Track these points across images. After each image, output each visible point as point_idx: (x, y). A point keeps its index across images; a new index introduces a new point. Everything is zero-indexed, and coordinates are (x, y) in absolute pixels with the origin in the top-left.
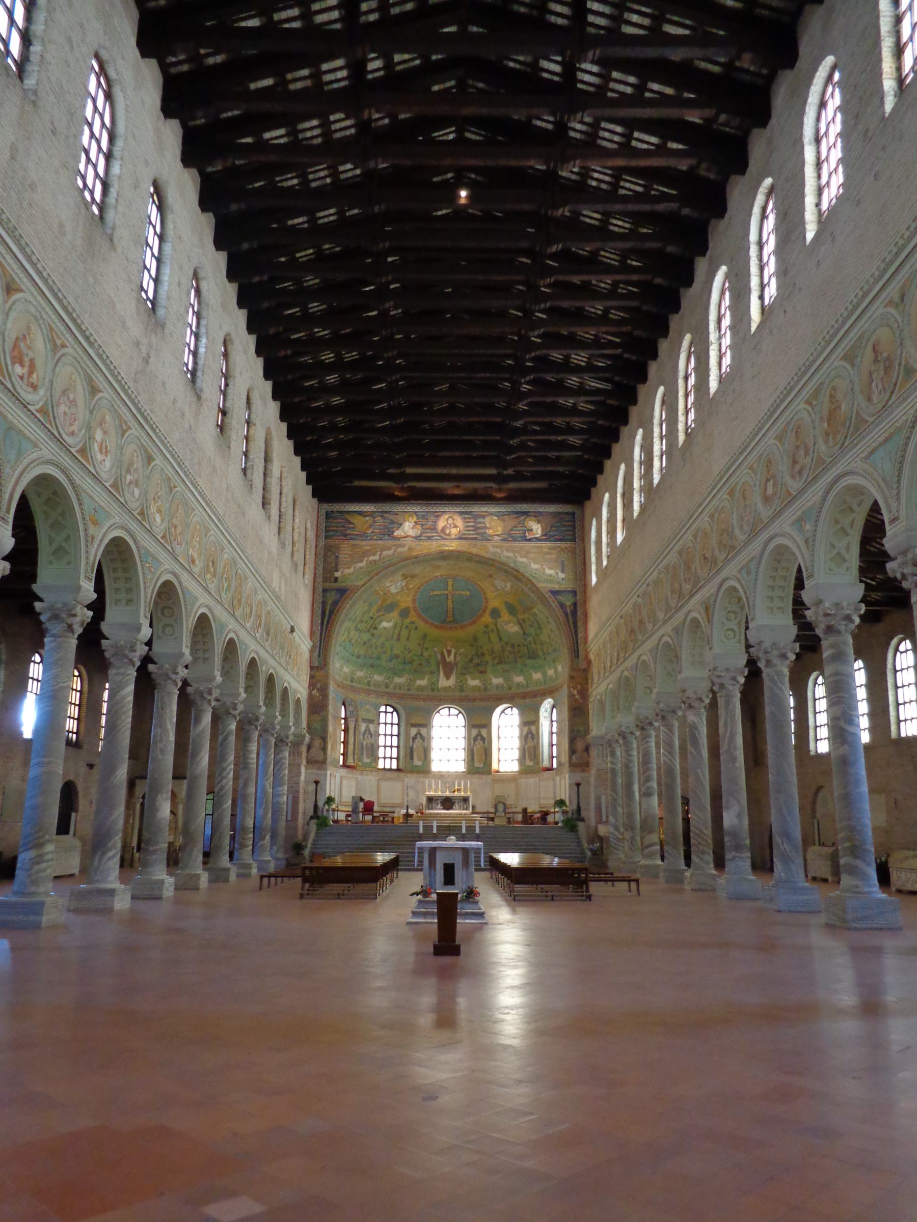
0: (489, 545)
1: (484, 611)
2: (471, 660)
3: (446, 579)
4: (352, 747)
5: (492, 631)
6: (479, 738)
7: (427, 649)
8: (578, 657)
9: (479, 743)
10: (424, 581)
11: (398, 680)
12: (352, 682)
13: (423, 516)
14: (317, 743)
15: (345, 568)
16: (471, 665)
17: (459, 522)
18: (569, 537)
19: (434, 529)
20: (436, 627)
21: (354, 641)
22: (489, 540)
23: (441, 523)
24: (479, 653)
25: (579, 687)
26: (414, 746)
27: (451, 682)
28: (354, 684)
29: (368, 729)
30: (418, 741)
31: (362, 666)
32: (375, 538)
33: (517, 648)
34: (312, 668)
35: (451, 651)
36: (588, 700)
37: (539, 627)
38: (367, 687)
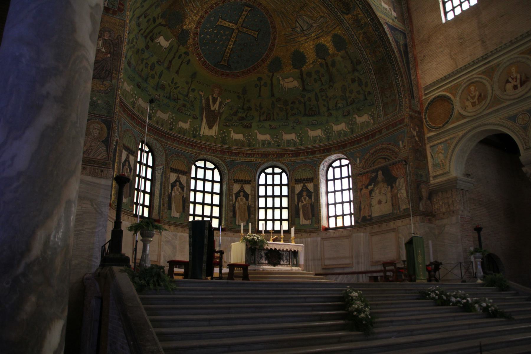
1: (263, 61)
2: (235, 114)
5: (266, 85)
6: (242, 194)
7: (193, 90)
8: (414, 98)
9: (242, 199)
25: (417, 128)
26: (173, 194)
27: (213, 132)
29: (127, 160)
30: (178, 190)
35: (217, 99)
36: (425, 144)
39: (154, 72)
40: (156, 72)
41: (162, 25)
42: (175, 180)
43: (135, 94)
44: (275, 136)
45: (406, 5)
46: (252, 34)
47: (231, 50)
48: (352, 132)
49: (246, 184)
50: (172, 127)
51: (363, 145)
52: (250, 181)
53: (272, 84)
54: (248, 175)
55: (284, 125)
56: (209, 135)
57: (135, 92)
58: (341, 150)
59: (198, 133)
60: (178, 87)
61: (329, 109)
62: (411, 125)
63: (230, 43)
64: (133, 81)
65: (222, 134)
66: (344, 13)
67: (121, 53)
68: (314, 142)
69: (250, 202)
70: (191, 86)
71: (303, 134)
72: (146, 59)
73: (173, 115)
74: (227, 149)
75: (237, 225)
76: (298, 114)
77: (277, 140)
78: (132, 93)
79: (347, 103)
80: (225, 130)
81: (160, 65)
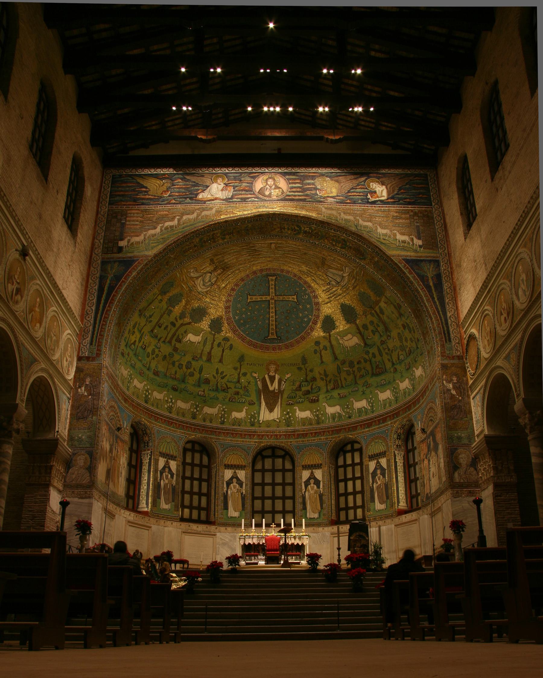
0: (320, 206)
1: (315, 323)
2: (299, 388)
3: (268, 275)
4: (146, 487)
6: (312, 481)
7: (245, 374)
8: (450, 341)
9: (312, 486)
10: (239, 277)
11: (208, 410)
12: (146, 402)
13: (235, 177)
14: (81, 460)
15: (132, 237)
16: (299, 393)
17: (282, 183)
18: (423, 201)
19: (250, 190)
20: (255, 346)
21: (149, 350)
22: (321, 202)
23: (259, 185)
24: (308, 379)
25: (455, 379)
26: (229, 492)
27: (276, 414)
28: (148, 406)
29: (167, 466)
30: (235, 487)
31: (162, 386)
32: (174, 202)
33: (357, 366)
34: (79, 359)
36: (469, 397)
37: (387, 329)
38: (168, 414)
39: (192, 370)
40: (194, 369)
41: (185, 324)
42: (230, 477)
43: (171, 399)
44: (346, 407)
45: (442, 221)
46: (290, 299)
47: (276, 321)
48: (414, 388)
49: (316, 468)
50: (224, 420)
51: (421, 405)
52: (321, 464)
53: (332, 346)
54: (319, 458)
55: (354, 391)
56: (270, 420)
57: (171, 397)
58: (407, 413)
59: (256, 420)
60: (226, 375)
61: (393, 364)
62: (444, 377)
63: (271, 315)
64: (166, 387)
65: (286, 415)
66: (360, 259)
67: (100, 393)
68: (385, 405)
69: (322, 490)
70: (240, 370)
71: (374, 399)
72: (178, 361)
73: (224, 407)
74: (293, 432)
75: (307, 518)
76: (366, 375)
77: (348, 410)
78: (166, 398)
79: (406, 353)
80: (288, 410)
81: (197, 360)
